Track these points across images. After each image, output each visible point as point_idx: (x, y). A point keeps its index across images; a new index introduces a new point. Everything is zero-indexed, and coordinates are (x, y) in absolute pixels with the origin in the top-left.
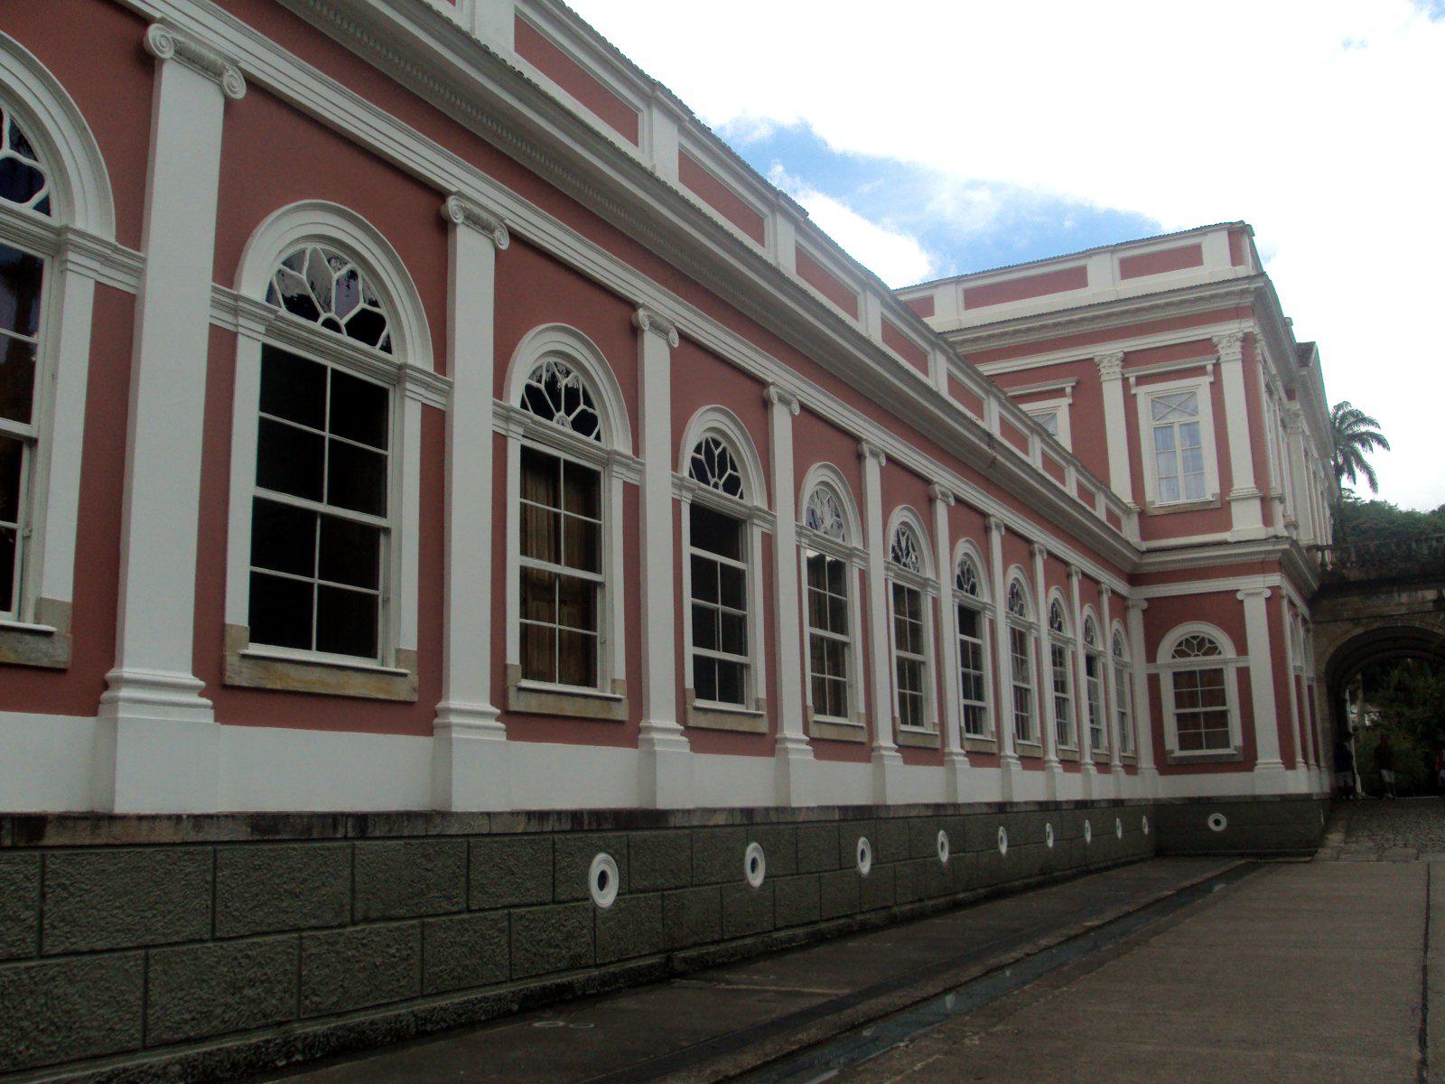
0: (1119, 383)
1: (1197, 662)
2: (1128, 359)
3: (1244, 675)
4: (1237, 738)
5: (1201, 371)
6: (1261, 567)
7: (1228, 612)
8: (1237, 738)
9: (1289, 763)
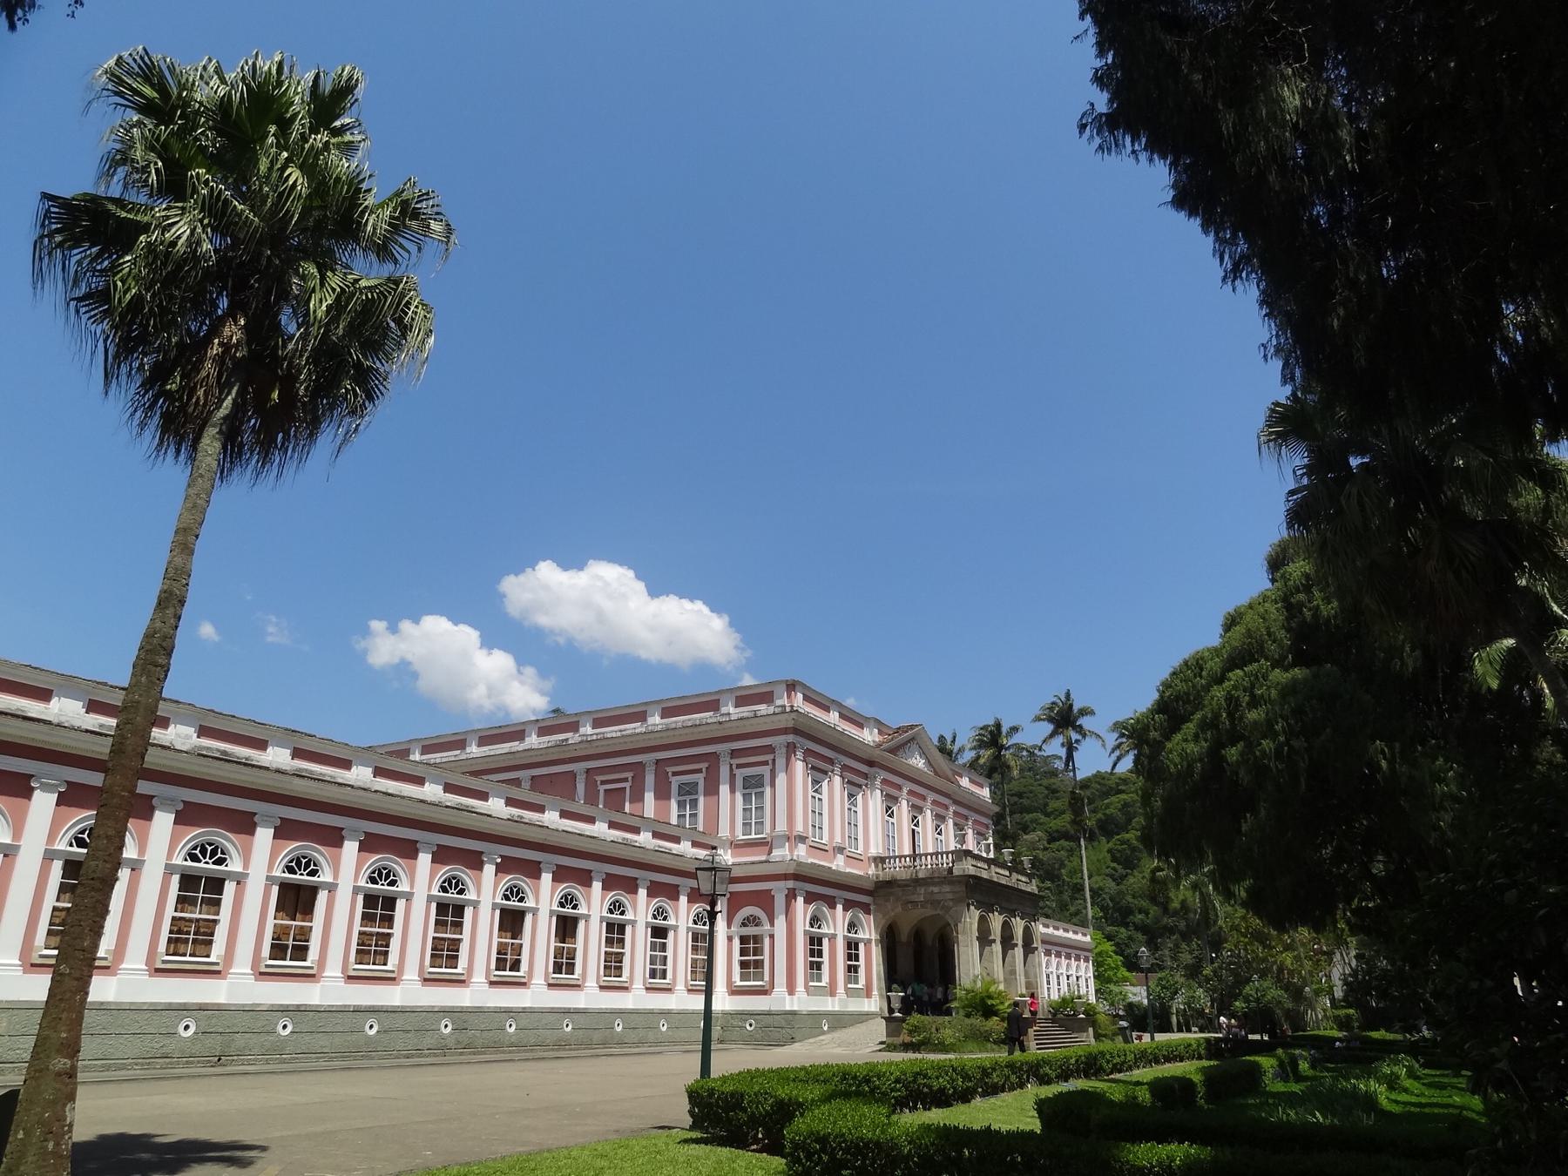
0: (728, 766)
1: (750, 931)
2: (734, 753)
3: (772, 936)
4: (767, 978)
5: (765, 763)
6: (785, 877)
8: (767, 978)
9: (791, 990)
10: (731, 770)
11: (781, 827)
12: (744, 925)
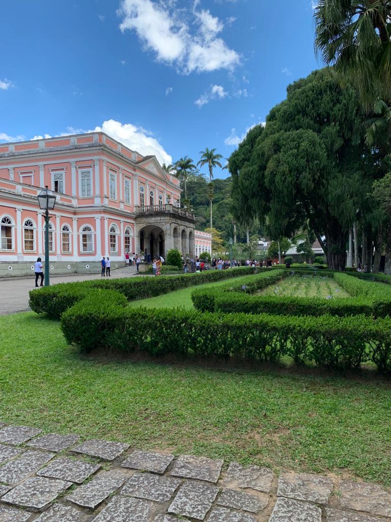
1: (87, 233)
3: (95, 235)
4: (93, 249)
5: (90, 167)
6: (100, 212)
7: (92, 221)
10: (76, 169)
11: (98, 192)
12: (84, 230)
